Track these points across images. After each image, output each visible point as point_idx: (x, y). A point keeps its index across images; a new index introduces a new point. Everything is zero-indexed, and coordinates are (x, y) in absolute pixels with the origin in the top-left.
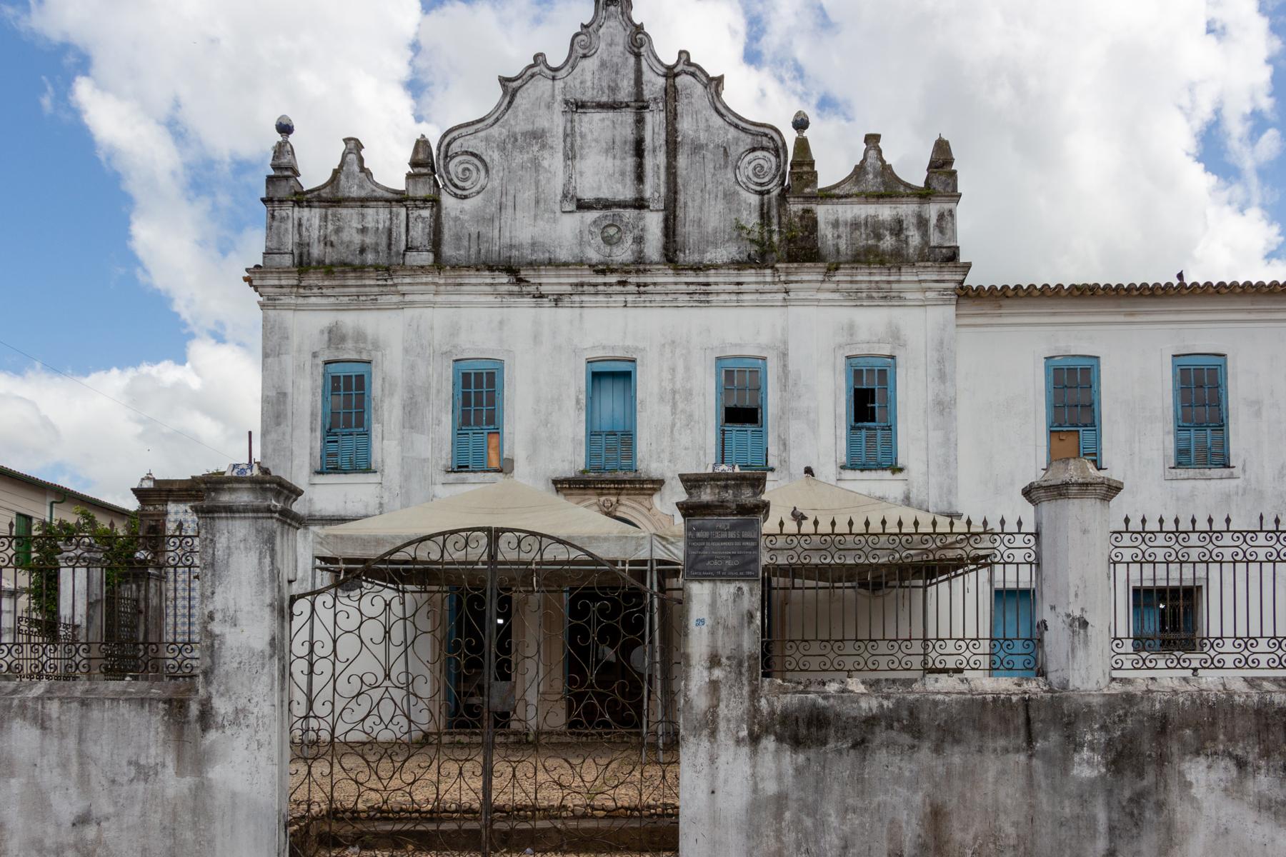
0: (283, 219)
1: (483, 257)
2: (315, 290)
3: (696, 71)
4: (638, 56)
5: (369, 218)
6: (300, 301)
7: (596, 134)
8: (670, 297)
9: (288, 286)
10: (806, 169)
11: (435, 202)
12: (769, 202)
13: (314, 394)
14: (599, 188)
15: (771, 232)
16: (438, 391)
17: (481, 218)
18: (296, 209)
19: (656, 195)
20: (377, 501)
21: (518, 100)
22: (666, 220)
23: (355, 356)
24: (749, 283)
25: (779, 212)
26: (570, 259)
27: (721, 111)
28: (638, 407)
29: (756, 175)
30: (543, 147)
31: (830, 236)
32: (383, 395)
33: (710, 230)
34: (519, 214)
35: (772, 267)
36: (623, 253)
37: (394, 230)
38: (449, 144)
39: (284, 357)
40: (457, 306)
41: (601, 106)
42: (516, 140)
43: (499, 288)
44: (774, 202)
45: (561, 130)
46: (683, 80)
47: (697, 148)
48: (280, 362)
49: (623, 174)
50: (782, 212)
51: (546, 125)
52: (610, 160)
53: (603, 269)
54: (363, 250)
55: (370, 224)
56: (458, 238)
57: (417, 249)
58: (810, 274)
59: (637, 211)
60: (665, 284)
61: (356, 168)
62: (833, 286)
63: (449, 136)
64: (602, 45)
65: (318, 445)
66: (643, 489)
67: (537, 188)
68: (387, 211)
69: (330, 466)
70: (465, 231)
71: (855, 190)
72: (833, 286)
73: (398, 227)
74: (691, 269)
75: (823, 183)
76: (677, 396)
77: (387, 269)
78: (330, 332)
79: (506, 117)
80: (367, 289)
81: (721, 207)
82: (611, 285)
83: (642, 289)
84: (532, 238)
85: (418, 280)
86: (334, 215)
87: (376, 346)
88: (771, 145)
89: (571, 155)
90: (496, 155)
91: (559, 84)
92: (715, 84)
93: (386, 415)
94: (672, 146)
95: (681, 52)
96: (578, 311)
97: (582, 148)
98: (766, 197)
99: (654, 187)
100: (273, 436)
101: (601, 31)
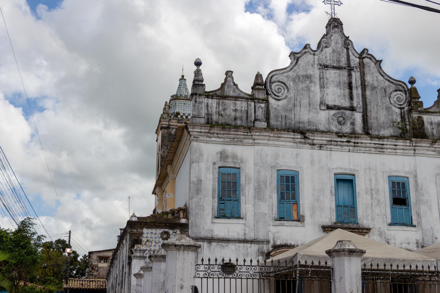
0: (200, 103)
1: (288, 126)
2: (215, 135)
3: (371, 57)
4: (348, 49)
5: (238, 105)
6: (208, 139)
7: (332, 79)
8: (367, 149)
9: (204, 132)
10: (417, 100)
11: (267, 101)
12: (404, 113)
13: (214, 181)
14: (335, 101)
15: (406, 125)
16: (270, 183)
17: (286, 109)
18: (206, 99)
19: (359, 106)
20: (243, 232)
21: (300, 62)
22: (363, 116)
23: (232, 165)
24: (399, 145)
25: (408, 117)
26: (325, 130)
27: (383, 74)
28: (357, 196)
29: (398, 101)
30: (311, 82)
31: (429, 128)
32: (246, 183)
33: (381, 122)
34: (302, 109)
35: (410, 140)
36: (347, 129)
37: (249, 111)
38: (272, 77)
39: (201, 164)
40: (278, 146)
41: (334, 68)
42: (300, 78)
43: (296, 140)
44: (406, 112)
45: (318, 75)
46: (366, 60)
47: (374, 88)
48: (199, 166)
49: (344, 96)
50: (410, 117)
51: (312, 73)
52: (339, 90)
53: (339, 135)
54: (235, 119)
55: (239, 108)
56: (277, 117)
57: (259, 120)
58: (425, 144)
59: (351, 112)
60: (366, 143)
61: (232, 84)
62: (433, 149)
63: (272, 74)
64: (333, 43)
65: (216, 204)
66: (363, 232)
67: (309, 99)
68: (246, 103)
69: (221, 215)
70: (279, 114)
71: (437, 110)
72: (433, 149)
73: (251, 110)
74: (377, 138)
75: (425, 106)
76: (373, 192)
77: (249, 128)
78: (221, 154)
79: (295, 68)
80: (238, 136)
81: (386, 112)
82: (343, 142)
83: (356, 144)
84: (308, 119)
85: (262, 134)
86: (223, 103)
87: (242, 161)
88: (403, 89)
89: (322, 87)
90: (291, 84)
91: (316, 57)
92: (378, 63)
93: (247, 193)
94: (364, 86)
95: (365, 49)
96: (329, 152)
97: (327, 84)
98: (403, 110)
99: (357, 102)
100: (195, 200)
101: (332, 38)
